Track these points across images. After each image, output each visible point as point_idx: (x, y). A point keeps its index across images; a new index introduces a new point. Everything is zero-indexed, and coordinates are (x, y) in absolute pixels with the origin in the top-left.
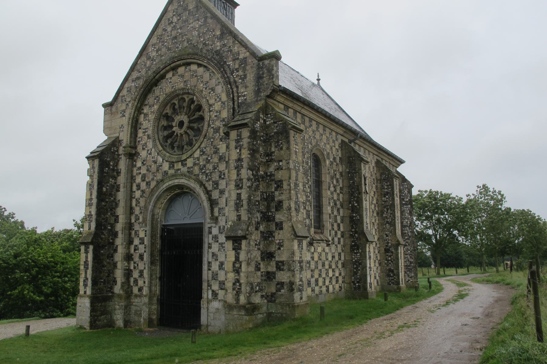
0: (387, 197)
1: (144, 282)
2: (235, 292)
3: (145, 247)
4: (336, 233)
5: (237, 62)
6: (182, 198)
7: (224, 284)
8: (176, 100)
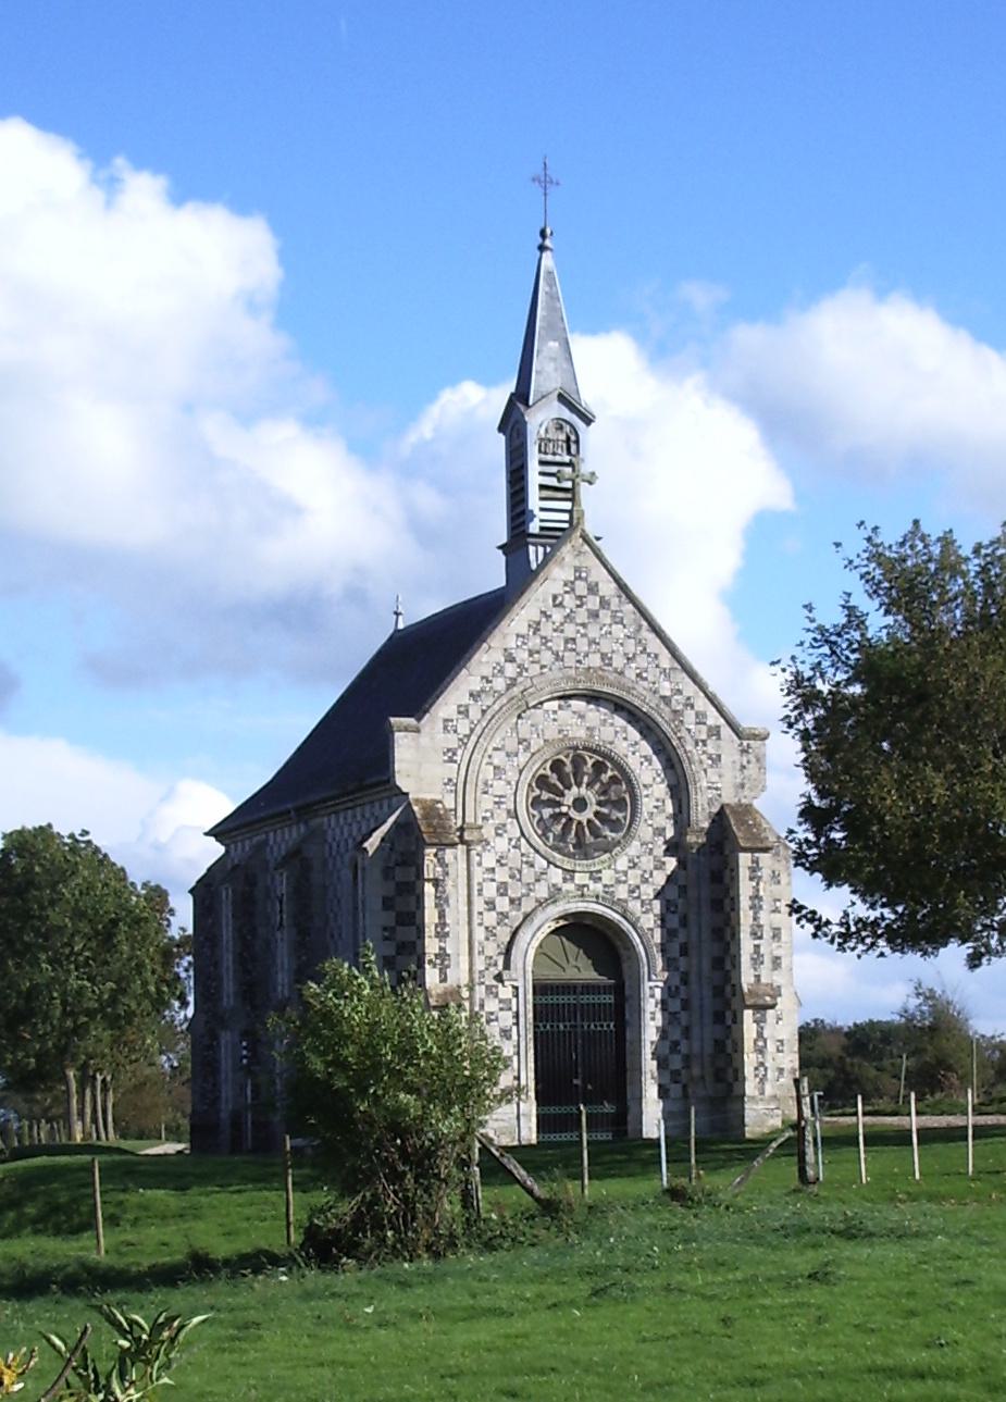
2: (758, 1080)
5: (704, 728)
7: (680, 1074)
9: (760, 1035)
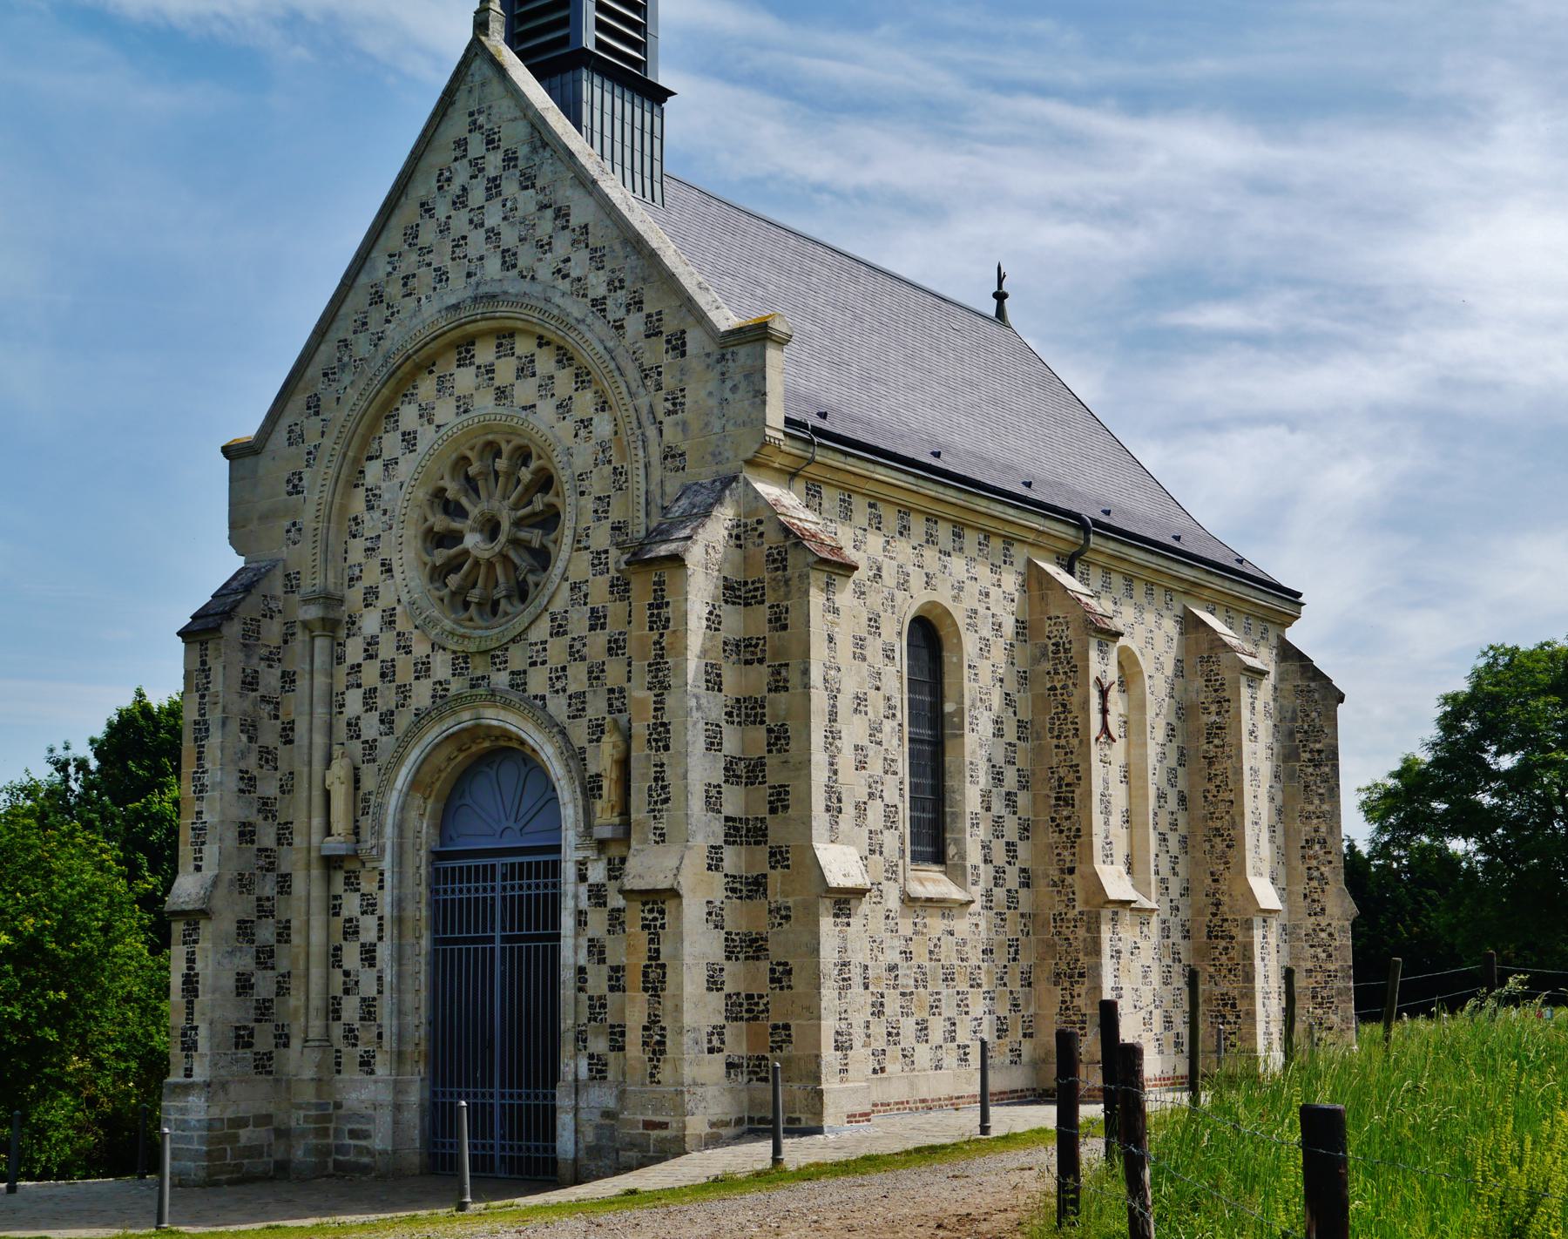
0: (1216, 741)
1: (380, 1036)
3: (381, 927)
4: (1000, 871)
6: (495, 767)
8: (472, 449)
9: (655, 955)
